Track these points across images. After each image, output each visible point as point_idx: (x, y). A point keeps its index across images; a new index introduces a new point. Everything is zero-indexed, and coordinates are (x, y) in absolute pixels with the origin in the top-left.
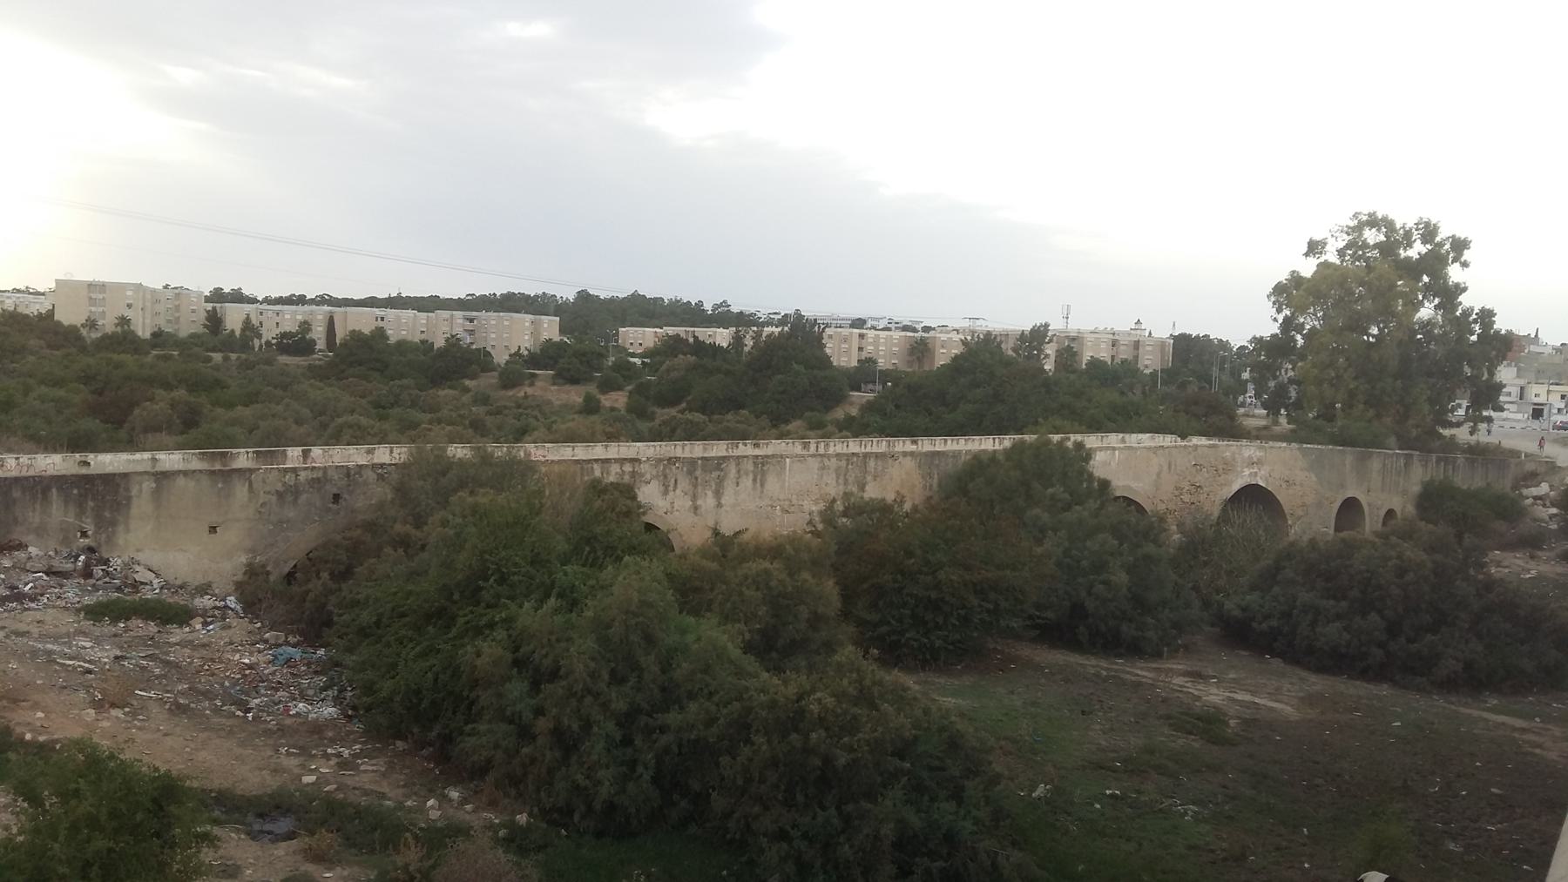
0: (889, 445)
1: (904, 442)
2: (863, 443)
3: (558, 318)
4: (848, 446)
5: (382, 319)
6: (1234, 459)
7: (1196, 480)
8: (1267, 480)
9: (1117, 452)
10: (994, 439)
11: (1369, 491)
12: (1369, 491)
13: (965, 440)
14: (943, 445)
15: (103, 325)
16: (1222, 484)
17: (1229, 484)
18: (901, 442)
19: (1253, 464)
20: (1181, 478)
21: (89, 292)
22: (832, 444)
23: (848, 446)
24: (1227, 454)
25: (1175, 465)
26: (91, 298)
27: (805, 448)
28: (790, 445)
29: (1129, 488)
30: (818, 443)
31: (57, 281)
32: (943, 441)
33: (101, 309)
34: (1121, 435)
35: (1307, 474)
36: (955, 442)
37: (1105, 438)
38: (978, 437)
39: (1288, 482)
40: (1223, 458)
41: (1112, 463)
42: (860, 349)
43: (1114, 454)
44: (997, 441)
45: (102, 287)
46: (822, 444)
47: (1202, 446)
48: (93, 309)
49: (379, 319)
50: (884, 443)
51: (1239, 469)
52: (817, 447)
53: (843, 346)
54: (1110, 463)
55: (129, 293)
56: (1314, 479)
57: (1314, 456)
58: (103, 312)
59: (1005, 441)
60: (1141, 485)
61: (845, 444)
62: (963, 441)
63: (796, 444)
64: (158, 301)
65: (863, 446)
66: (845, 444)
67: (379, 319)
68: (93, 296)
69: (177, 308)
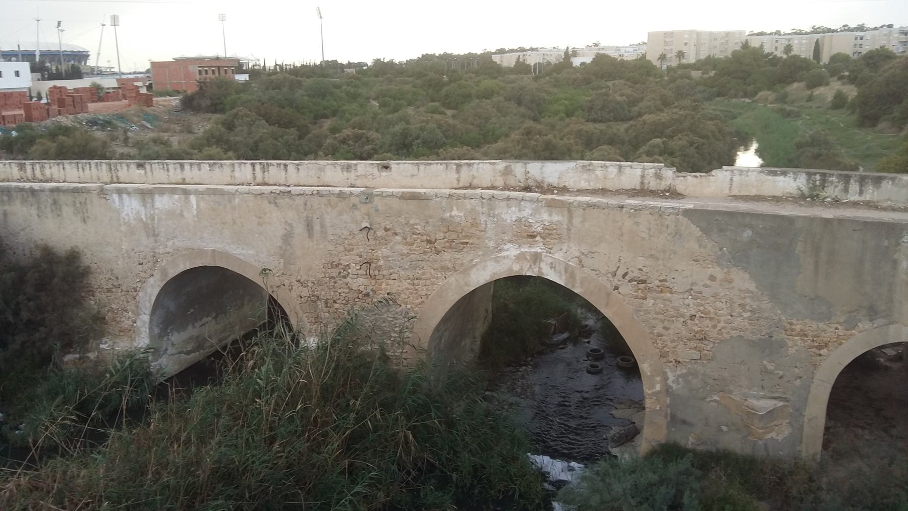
0: (111, 169)
1: (128, 166)
2: (80, 165)
4: (64, 168)
5: (862, 38)
6: (475, 224)
8: (572, 276)
9: (193, 199)
10: (253, 165)
13: (210, 165)
14: (179, 170)
15: (671, 57)
16: (445, 269)
17: (466, 271)
18: (124, 165)
19: (534, 237)
20: (341, 248)
21: (665, 37)
22: (47, 166)
23: (64, 168)
24: (455, 212)
26: (665, 41)
27: (21, 168)
28: (7, 166)
29: (226, 255)
30: (33, 164)
31: (648, 33)
32: (178, 166)
34: (501, 165)
35: (718, 272)
36: (195, 168)
39: (644, 282)
40: (443, 220)
41: (185, 214)
43: (187, 201)
44: (258, 167)
45: (672, 34)
46: (37, 165)
47: (381, 195)
48: (666, 48)
49: (859, 38)
50: (104, 167)
51: (491, 244)
52: (33, 169)
54: (182, 215)
55: (686, 36)
56: (752, 286)
58: (672, 49)
59: (271, 168)
60: (251, 252)
61: (61, 166)
63: (13, 165)
64: (716, 39)
65: (80, 170)
66: (61, 166)
67: (859, 38)
68: (667, 40)
69: (727, 42)
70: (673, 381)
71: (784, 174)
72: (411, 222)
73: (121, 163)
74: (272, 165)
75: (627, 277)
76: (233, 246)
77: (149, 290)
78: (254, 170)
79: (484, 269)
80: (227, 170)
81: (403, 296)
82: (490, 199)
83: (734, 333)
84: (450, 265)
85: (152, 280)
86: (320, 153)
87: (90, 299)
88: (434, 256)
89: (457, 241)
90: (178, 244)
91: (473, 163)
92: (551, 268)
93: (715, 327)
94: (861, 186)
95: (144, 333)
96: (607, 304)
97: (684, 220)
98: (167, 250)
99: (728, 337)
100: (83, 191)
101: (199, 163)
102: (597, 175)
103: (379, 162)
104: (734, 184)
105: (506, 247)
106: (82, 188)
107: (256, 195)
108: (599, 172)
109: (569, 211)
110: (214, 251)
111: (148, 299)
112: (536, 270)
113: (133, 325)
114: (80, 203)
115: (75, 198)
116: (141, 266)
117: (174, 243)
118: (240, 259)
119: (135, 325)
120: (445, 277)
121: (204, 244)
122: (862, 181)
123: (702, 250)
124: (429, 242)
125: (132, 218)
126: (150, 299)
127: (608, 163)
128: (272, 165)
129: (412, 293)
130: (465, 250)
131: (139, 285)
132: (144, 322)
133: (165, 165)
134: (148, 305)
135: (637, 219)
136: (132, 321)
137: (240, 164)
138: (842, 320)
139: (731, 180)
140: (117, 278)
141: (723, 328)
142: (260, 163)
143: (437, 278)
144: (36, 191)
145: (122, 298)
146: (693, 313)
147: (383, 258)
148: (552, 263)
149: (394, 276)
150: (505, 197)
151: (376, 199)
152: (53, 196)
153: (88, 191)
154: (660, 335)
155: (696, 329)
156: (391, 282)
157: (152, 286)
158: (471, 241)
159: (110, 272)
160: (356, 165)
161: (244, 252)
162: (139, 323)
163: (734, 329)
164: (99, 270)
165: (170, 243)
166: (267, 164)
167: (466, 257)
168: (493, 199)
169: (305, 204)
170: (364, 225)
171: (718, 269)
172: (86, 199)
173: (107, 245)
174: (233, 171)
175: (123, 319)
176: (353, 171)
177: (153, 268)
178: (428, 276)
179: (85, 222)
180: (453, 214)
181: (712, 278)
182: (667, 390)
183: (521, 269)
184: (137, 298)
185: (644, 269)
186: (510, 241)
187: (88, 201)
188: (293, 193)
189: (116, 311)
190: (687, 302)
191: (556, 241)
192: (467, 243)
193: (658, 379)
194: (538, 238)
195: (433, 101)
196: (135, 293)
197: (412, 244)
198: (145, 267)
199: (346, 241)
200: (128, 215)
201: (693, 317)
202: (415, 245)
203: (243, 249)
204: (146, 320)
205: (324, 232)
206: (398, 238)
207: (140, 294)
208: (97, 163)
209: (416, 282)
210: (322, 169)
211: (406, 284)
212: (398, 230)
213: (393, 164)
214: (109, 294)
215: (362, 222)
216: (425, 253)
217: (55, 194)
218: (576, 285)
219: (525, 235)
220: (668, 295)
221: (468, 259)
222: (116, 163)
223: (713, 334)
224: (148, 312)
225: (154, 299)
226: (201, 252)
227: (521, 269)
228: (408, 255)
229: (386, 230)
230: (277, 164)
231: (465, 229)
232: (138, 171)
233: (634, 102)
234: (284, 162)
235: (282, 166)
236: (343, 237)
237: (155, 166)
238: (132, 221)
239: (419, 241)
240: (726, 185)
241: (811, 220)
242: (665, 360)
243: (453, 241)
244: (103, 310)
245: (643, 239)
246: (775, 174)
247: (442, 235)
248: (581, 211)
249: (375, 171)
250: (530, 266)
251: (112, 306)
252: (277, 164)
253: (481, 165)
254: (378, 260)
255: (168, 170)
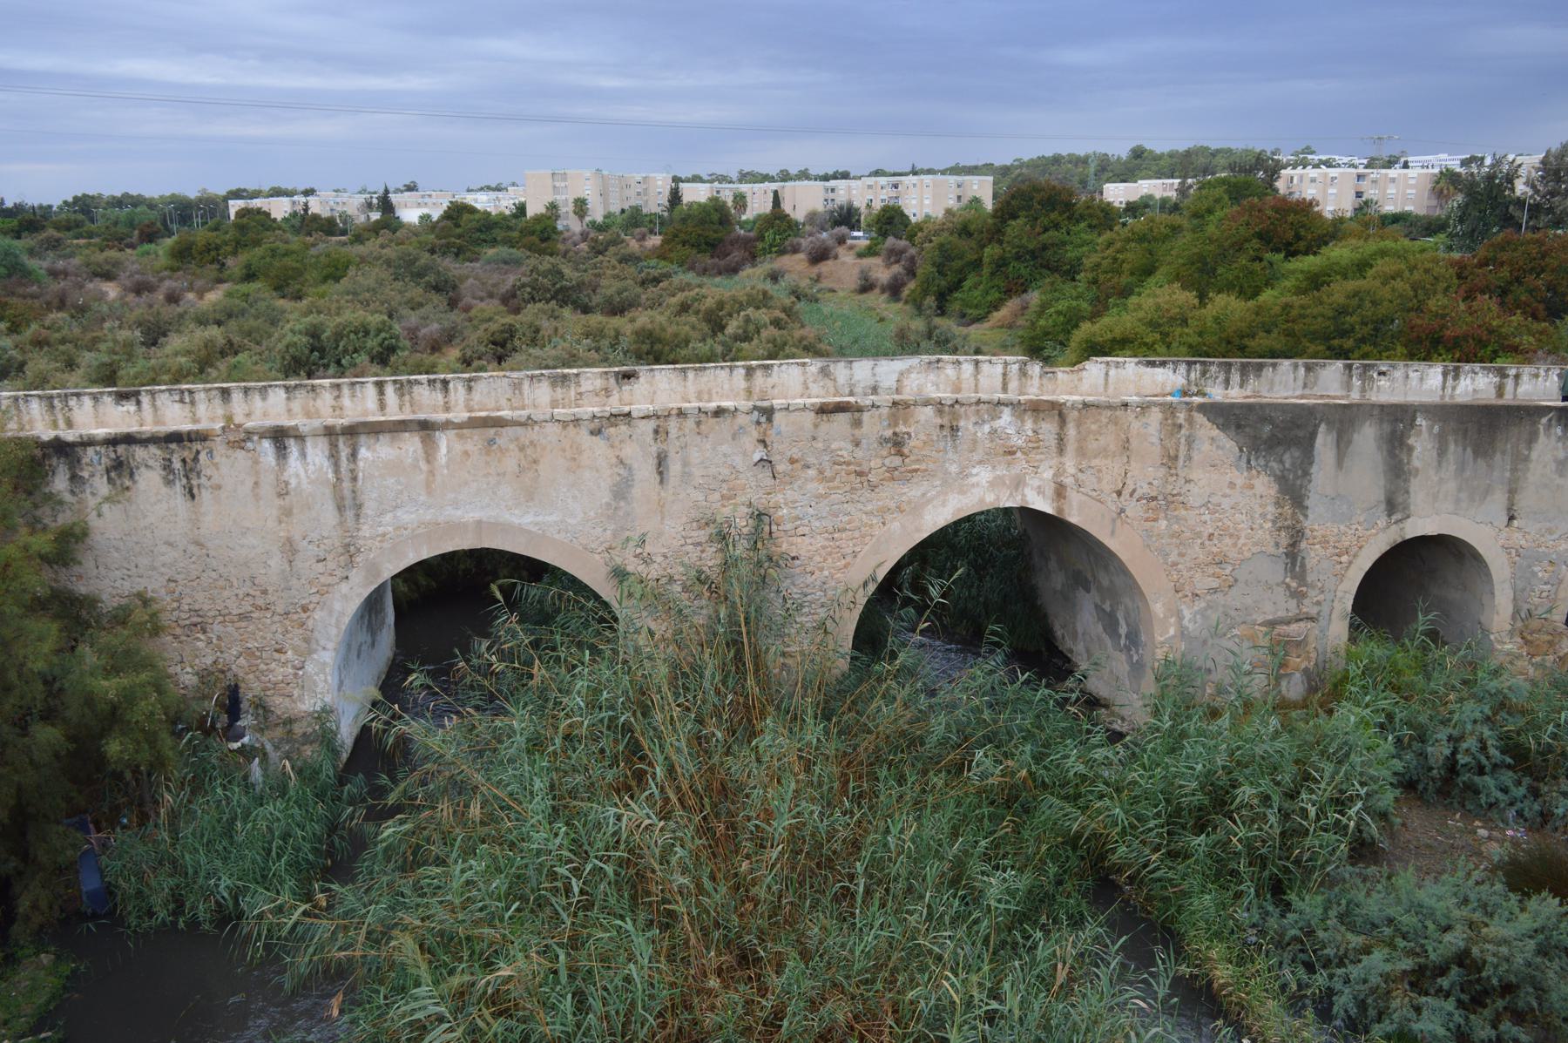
0: (52, 407)
3: (991, 179)
5: (833, 190)
7: (779, 498)
10: (380, 386)
11: (1511, 518)
12: (1511, 518)
13: (287, 388)
14: (218, 401)
17: (917, 508)
20: (717, 496)
25: (685, 464)
26: (555, 187)
33: (564, 197)
37: (759, 373)
38: (326, 382)
42: (1359, 194)
44: (390, 390)
53: (1330, 191)
57: (1268, 428)
62: (282, 394)
68: (557, 184)
70: (1190, 621)
71: (1163, 364)
72: (833, 446)
73: (78, 395)
74: (418, 382)
75: (1136, 495)
76: (516, 512)
77: (337, 606)
78: (381, 393)
79: (944, 504)
80: (327, 398)
81: (818, 559)
82: (952, 406)
83: (1254, 550)
84: (892, 505)
85: (344, 587)
86: (302, 373)
87: (198, 639)
88: (868, 494)
89: (903, 469)
90: (407, 516)
91: (772, 365)
92: (1039, 493)
93: (1235, 545)
94: (1242, 375)
95: (321, 685)
96: (1113, 533)
97: (1200, 418)
98: (381, 530)
99: (1249, 555)
100: (193, 436)
101: (265, 387)
102: (947, 376)
103: (616, 369)
104: (1110, 381)
105: (974, 471)
106: (189, 433)
107: (564, 424)
108: (950, 371)
109: (1061, 415)
110: (479, 523)
111: (333, 621)
112: (1019, 498)
113: (296, 674)
114: (184, 461)
115: (172, 452)
116: (320, 564)
117: (395, 517)
118: (530, 532)
119: (301, 673)
120: (884, 523)
121: (459, 513)
122: (1244, 370)
123: (1220, 452)
124: (860, 474)
125: (304, 481)
126: (338, 621)
127: (961, 358)
128: (418, 382)
129: (830, 554)
130: (915, 480)
131: (315, 599)
132: (325, 664)
133: (186, 394)
134: (333, 631)
135: (1144, 420)
136: (294, 667)
137: (353, 384)
138: (1362, 519)
139: (1107, 374)
140: (265, 592)
141: (1244, 545)
142: (395, 382)
143: (871, 526)
144: (72, 445)
145: (274, 628)
146: (1211, 531)
147: (786, 504)
148: (1039, 487)
149: (806, 530)
150: (973, 400)
151: (777, 417)
152: (115, 451)
153: (202, 437)
154: (1175, 564)
155: (1215, 550)
156: (799, 540)
157: (345, 597)
158: (923, 467)
159: (248, 583)
160: (577, 375)
161: (540, 519)
162: (310, 668)
163: (1256, 544)
164: (221, 583)
165: (388, 518)
166: (409, 382)
167: (913, 491)
168: (957, 406)
169: (656, 432)
170: (757, 457)
171: (1237, 473)
172: (198, 452)
173: (244, 534)
174: (338, 397)
175: (273, 665)
176: (573, 386)
177: (351, 563)
178: (857, 524)
179: (193, 497)
180: (897, 430)
181: (1232, 485)
182: (1182, 633)
183: (998, 499)
184: (310, 623)
185: (1155, 482)
186: (980, 462)
187: (202, 457)
188: (634, 414)
189: (258, 654)
190: (1203, 518)
191: (1042, 456)
192: (916, 471)
193: (1173, 620)
194: (1019, 454)
195: (220, 281)
196: (304, 615)
197: (832, 479)
198: (331, 565)
199: (724, 485)
200: (297, 476)
201: (1211, 536)
202: (838, 479)
203: (536, 514)
204: (328, 660)
205: (686, 476)
206: (812, 472)
207: (318, 615)
208: (16, 399)
209: (836, 536)
210: (517, 386)
211: (820, 541)
212: (811, 460)
213: (642, 369)
214: (243, 624)
215: (754, 452)
216: (853, 489)
217: (121, 449)
218: (1075, 512)
219: (1001, 451)
220: (1184, 512)
221: (919, 494)
222: (66, 395)
223: (1233, 554)
224: (331, 645)
225: (347, 620)
226: (454, 527)
227: (998, 499)
228: (826, 496)
229: (792, 461)
230: (429, 381)
231: (916, 451)
232: (120, 408)
233: (580, 286)
234: (442, 376)
235: (438, 385)
236: (721, 478)
237: (164, 400)
238: (305, 485)
239: (843, 473)
240: (1101, 381)
241: (1324, 405)
242: (1180, 594)
243: (896, 469)
244: (226, 655)
245: (1153, 444)
246: (1152, 364)
247: (879, 461)
248: (1076, 413)
249: (612, 381)
250: (1011, 494)
251: (250, 645)
252: (429, 381)
253: (784, 367)
254: (778, 507)
255: (193, 403)
